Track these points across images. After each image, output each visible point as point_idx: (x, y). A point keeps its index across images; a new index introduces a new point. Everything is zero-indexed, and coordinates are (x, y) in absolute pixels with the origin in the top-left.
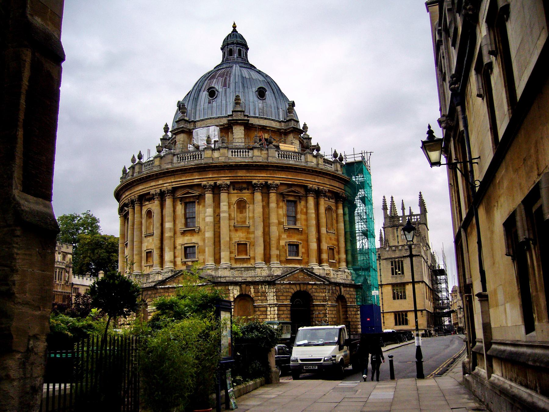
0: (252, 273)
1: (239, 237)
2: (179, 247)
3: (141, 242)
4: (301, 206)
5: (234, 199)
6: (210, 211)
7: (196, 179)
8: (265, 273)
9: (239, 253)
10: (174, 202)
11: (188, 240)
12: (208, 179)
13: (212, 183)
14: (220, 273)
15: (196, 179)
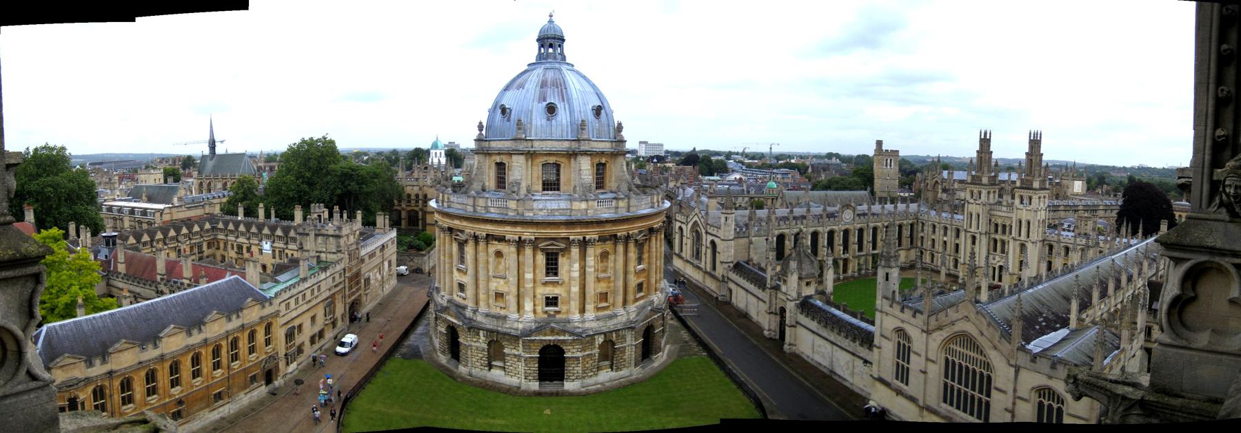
0: (615, 321)
1: (602, 287)
2: (539, 296)
3: (488, 281)
4: (646, 247)
5: (599, 251)
6: (576, 266)
7: (563, 232)
8: (624, 319)
9: (601, 301)
10: (535, 248)
11: (551, 291)
12: (575, 234)
13: (581, 238)
14: (587, 325)
15: (563, 232)
